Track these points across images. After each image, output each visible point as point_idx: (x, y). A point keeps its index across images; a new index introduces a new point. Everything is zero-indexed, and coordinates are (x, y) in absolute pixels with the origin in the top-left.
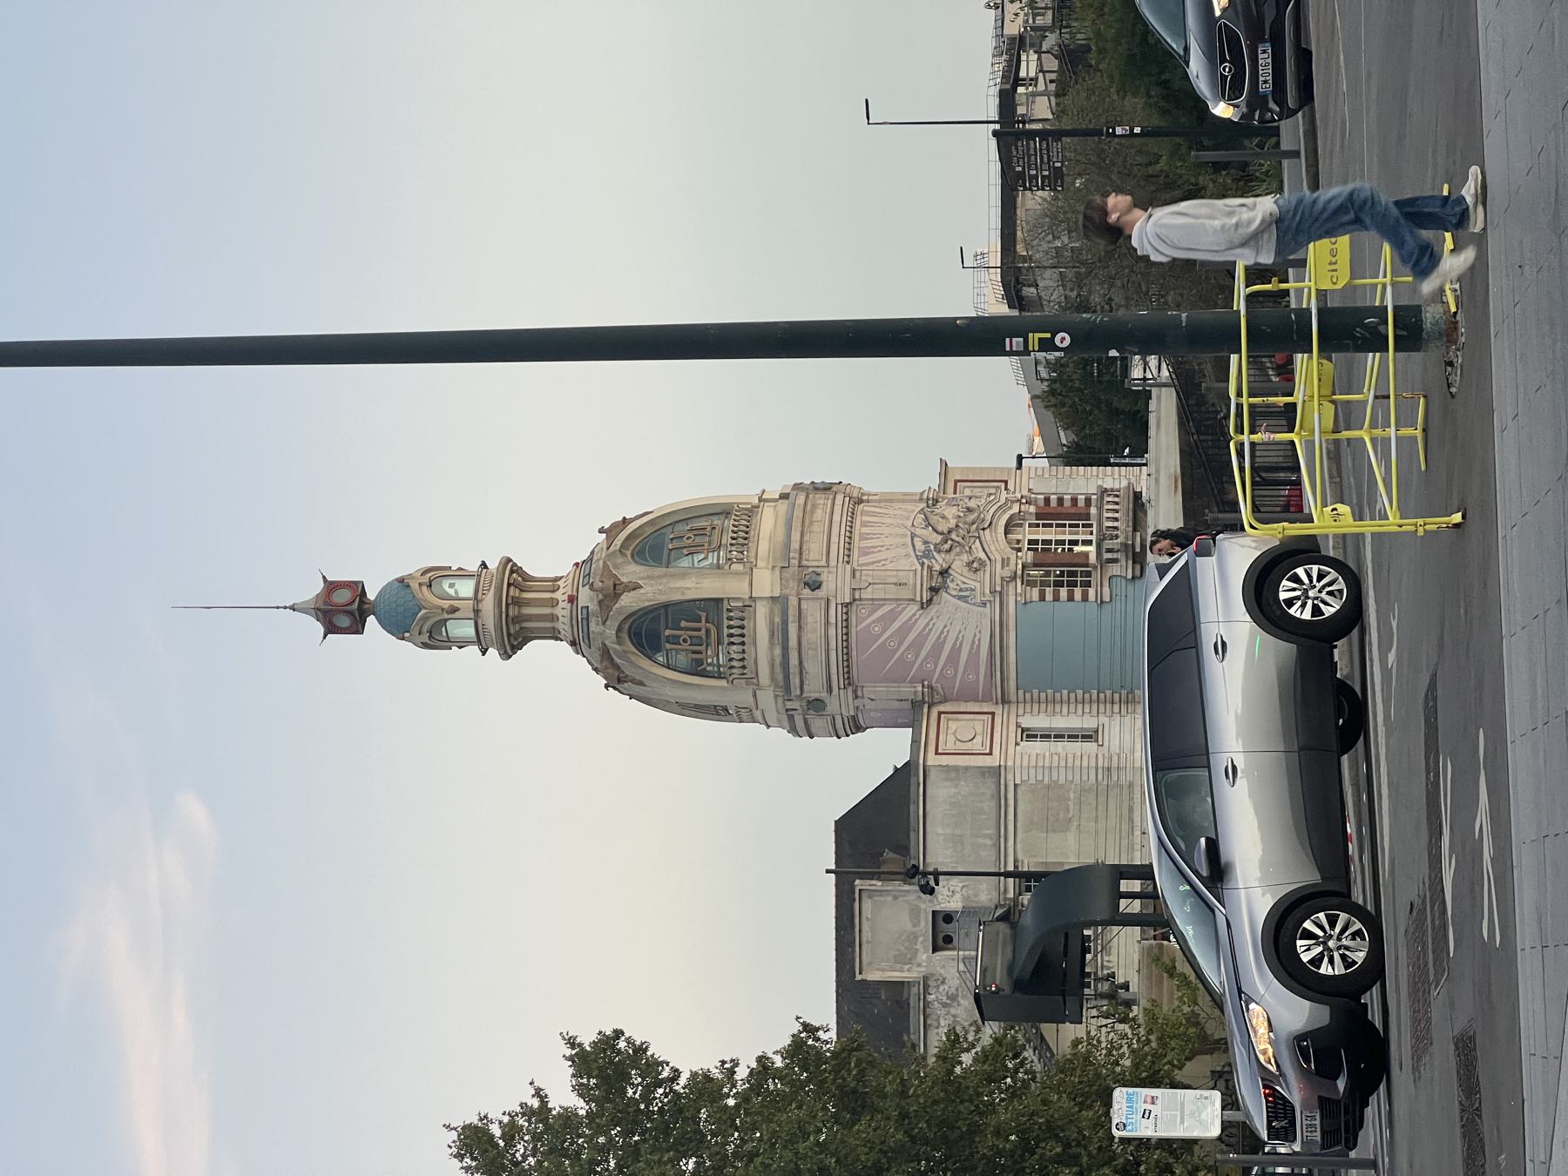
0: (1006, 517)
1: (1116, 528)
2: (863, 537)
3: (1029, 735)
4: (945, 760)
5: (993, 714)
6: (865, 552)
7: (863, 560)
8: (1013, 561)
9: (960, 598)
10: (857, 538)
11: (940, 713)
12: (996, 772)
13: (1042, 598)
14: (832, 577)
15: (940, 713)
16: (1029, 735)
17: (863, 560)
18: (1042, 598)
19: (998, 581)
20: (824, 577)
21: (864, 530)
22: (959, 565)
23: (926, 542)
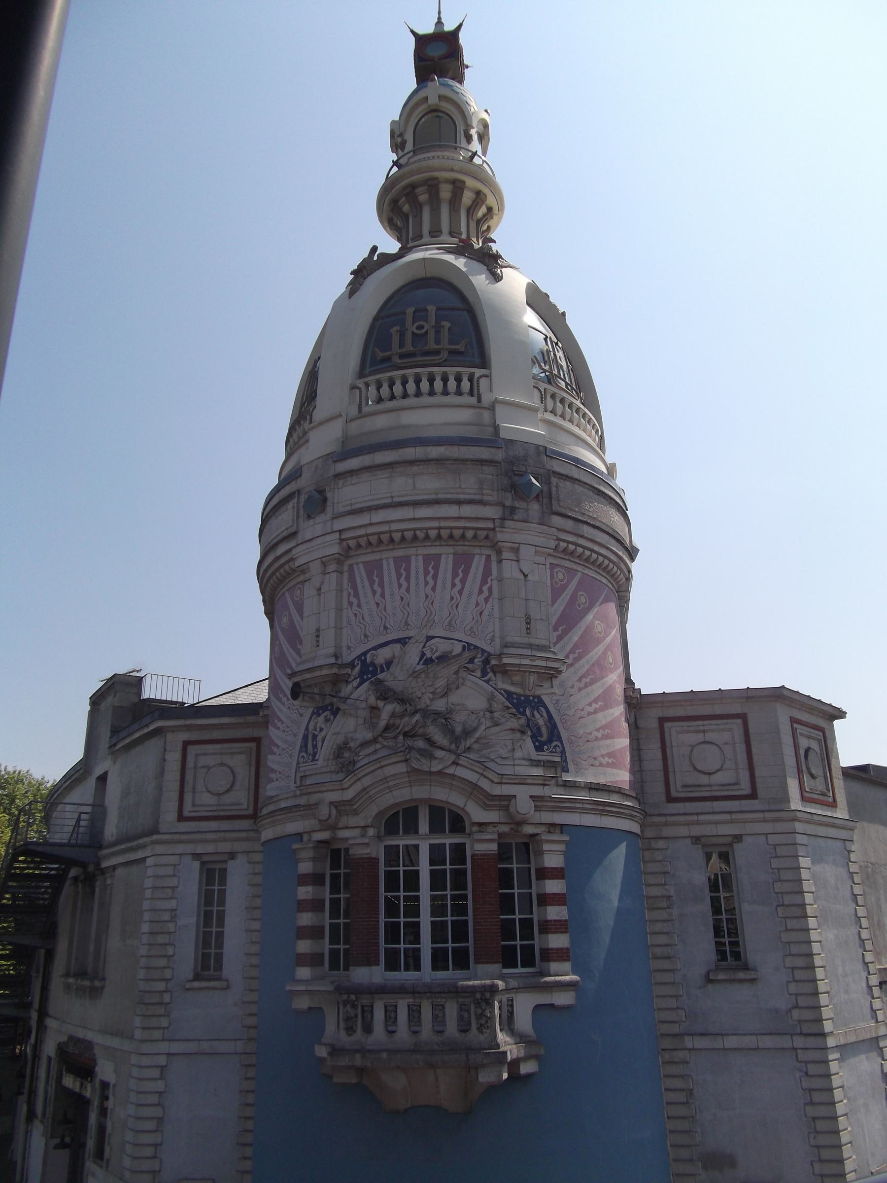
0: (456, 799)
1: (368, 1029)
2: (402, 563)
3: (213, 874)
4: (174, 758)
5: (254, 816)
6: (374, 569)
7: (360, 573)
8: (353, 821)
9: (305, 737)
10: (400, 553)
11: (258, 740)
12: (155, 830)
13: (303, 880)
14: (319, 530)
15: (258, 740)
16: (213, 874)
17: (360, 573)
18: (303, 880)
19: (314, 798)
20: (320, 518)
21: (417, 564)
22: (348, 727)
23: (389, 663)
